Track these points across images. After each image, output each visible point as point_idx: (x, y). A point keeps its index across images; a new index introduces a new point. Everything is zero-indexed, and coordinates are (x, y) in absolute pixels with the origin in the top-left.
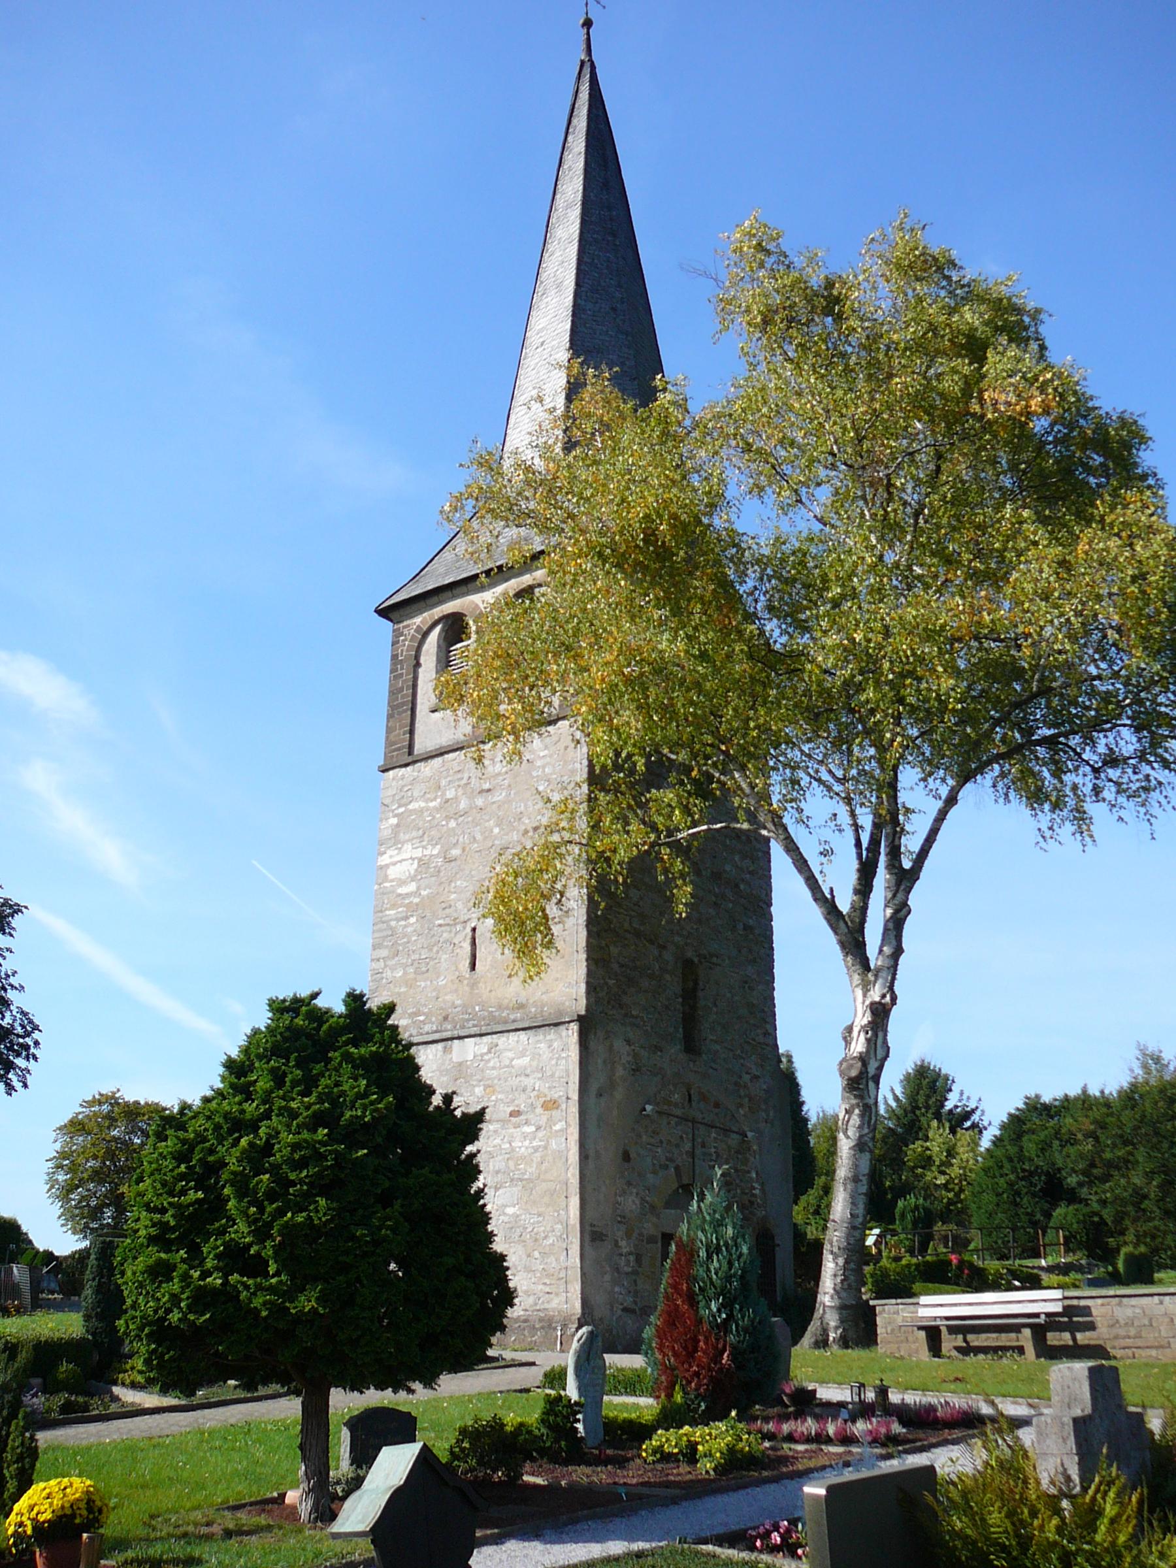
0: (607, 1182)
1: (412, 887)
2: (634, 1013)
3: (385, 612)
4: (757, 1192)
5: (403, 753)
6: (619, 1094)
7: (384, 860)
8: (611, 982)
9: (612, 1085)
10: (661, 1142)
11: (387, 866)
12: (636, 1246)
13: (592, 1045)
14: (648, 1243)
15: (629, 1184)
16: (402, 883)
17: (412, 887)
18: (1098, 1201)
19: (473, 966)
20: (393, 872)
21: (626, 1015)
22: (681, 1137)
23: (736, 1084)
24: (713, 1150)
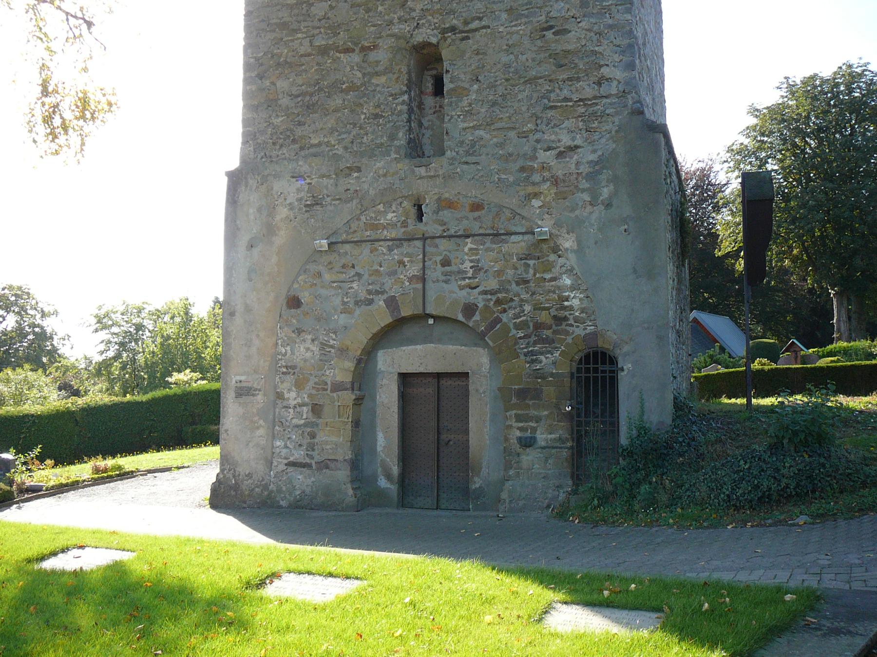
0: (262, 334)
2: (315, 141)
4: (576, 303)
6: (281, 238)
8: (277, 121)
9: (270, 230)
10: (359, 275)
12: (310, 396)
13: (242, 197)
14: (332, 391)
15: (299, 331)
18: (569, 296)
21: (302, 148)
22: (401, 263)
23: (522, 169)
24: (468, 264)
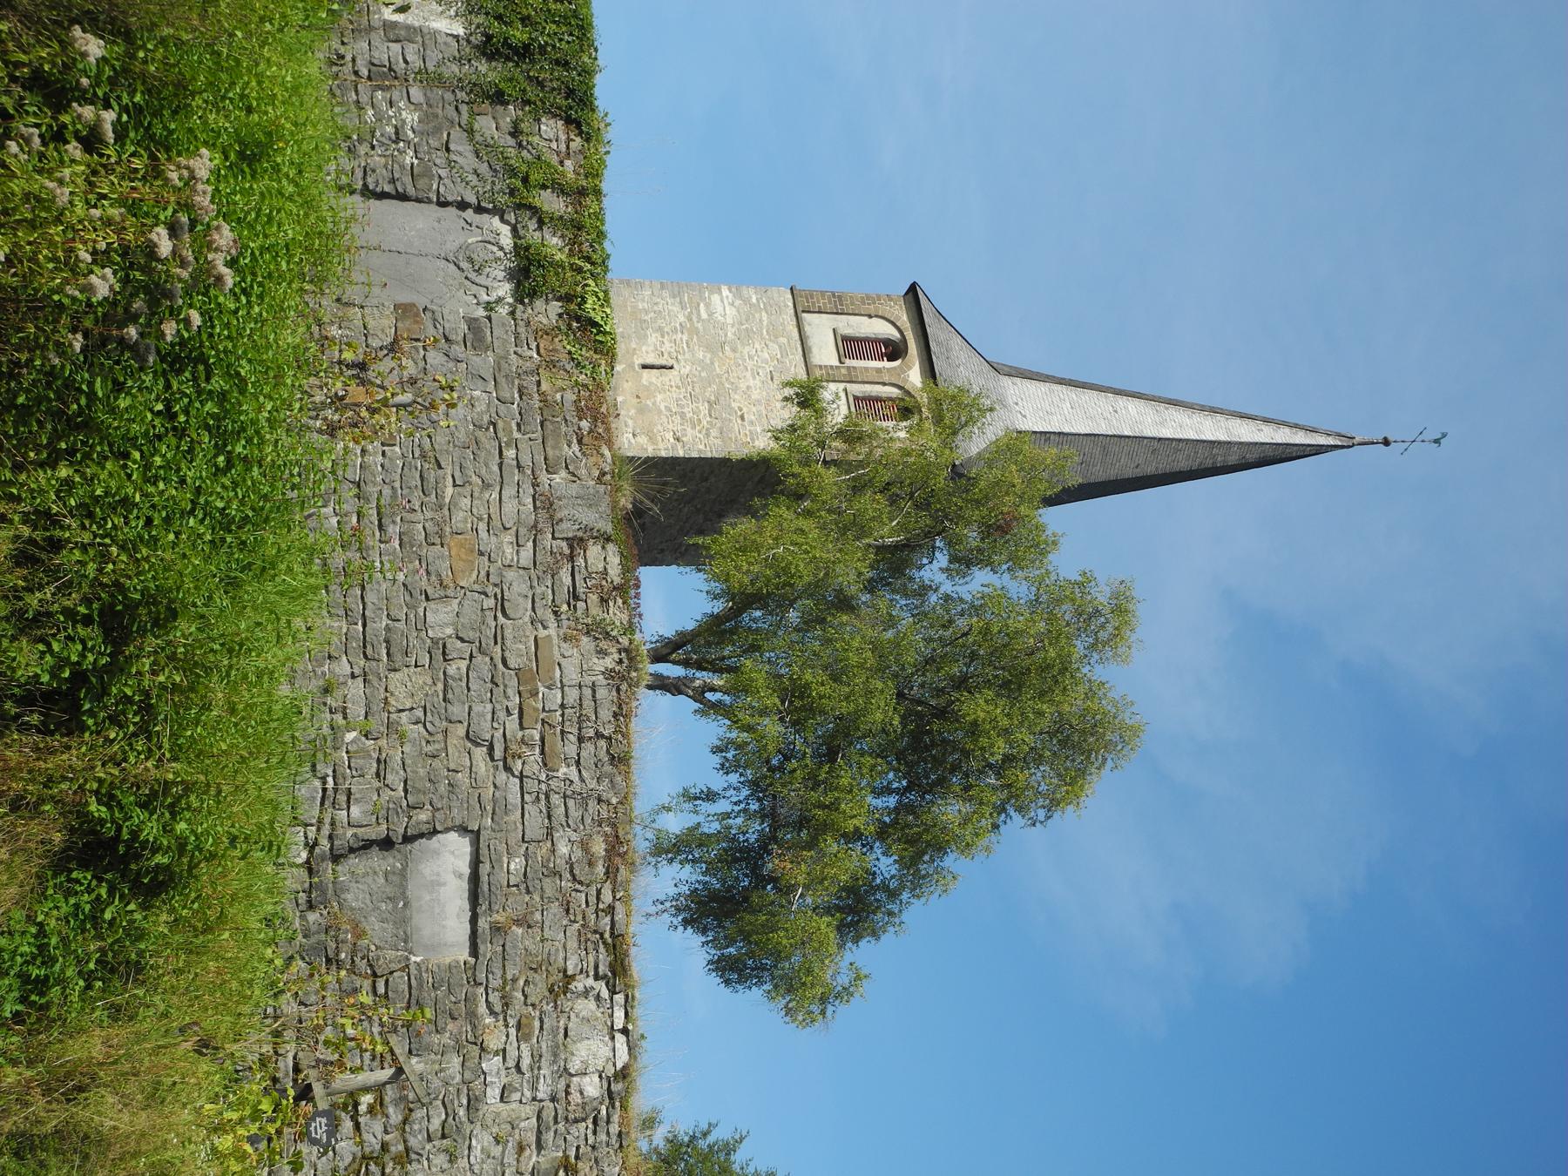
1: (704, 315)
3: (913, 289)
5: (803, 304)
7: (725, 292)
11: (720, 293)
16: (708, 306)
17: (704, 315)
19: (645, 367)
20: (715, 298)
